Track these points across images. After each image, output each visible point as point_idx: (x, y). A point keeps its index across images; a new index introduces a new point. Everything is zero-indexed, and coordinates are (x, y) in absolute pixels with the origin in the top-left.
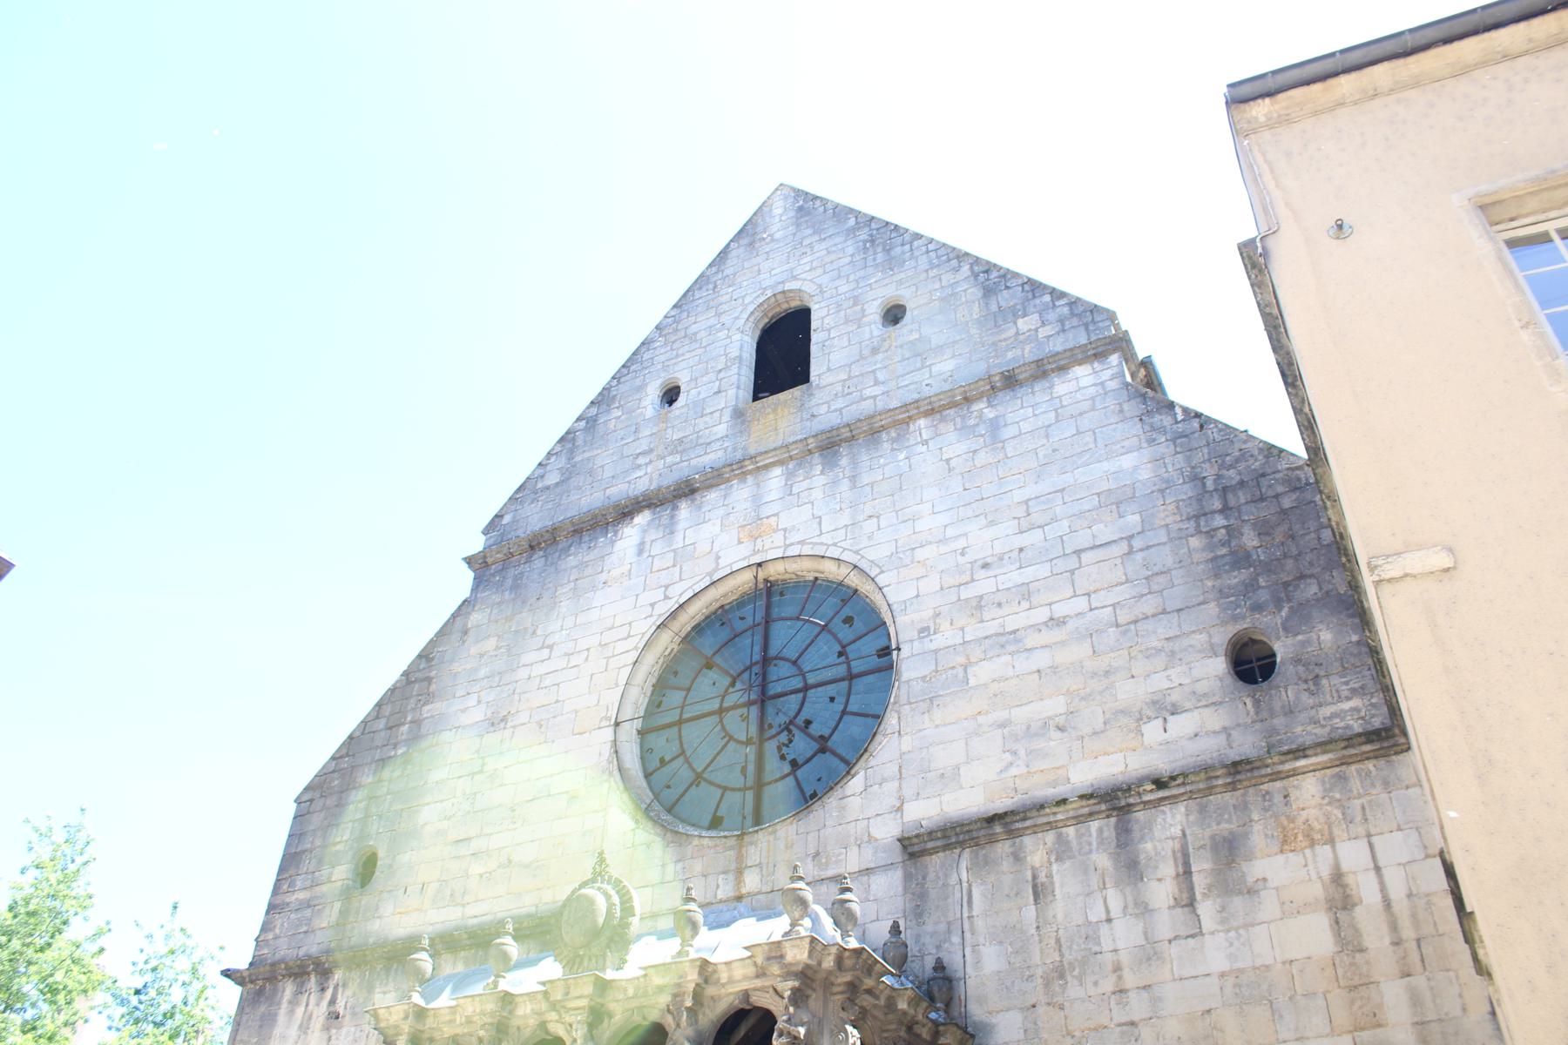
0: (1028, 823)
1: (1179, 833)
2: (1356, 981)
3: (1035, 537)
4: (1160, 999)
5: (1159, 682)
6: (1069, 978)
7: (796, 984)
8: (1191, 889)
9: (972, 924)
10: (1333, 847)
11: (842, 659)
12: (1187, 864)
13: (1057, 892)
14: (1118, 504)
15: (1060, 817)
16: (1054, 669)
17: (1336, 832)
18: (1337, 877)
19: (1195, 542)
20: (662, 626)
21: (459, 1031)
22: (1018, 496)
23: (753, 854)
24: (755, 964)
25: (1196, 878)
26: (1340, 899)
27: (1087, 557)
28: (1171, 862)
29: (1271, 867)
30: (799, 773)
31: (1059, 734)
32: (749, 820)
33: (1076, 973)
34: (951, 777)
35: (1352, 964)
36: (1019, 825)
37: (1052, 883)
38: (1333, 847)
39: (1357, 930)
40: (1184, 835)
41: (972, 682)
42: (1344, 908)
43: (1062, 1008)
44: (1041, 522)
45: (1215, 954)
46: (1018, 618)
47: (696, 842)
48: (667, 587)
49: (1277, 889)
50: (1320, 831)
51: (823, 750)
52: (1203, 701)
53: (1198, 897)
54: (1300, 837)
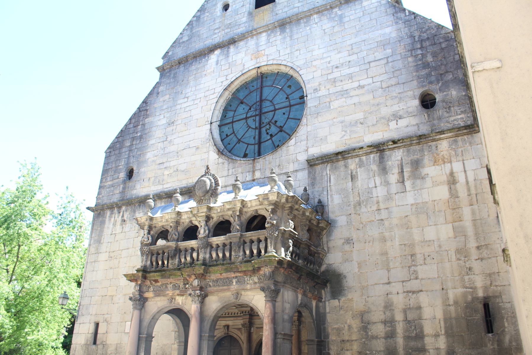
0: (350, 155)
2: (455, 207)
3: (354, 57)
5: (396, 108)
7: (273, 207)
8: (403, 177)
9: (330, 188)
10: (451, 164)
11: (287, 100)
12: (402, 169)
13: (359, 178)
14: (384, 45)
15: (360, 153)
16: (360, 103)
17: (452, 159)
18: (452, 174)
19: (410, 59)
20: (225, 89)
21: (164, 224)
22: (349, 42)
23: (258, 165)
24: (259, 201)
26: (452, 181)
27: (372, 64)
28: (397, 169)
29: (430, 170)
30: (273, 138)
31: (361, 125)
32: (257, 154)
33: (364, 204)
34: (324, 140)
35: (454, 202)
36: (346, 156)
38: (451, 164)
39: (457, 191)
40: (402, 159)
41: (332, 107)
42: (453, 184)
43: (359, 215)
44: (356, 52)
45: (410, 198)
46: (348, 85)
47: (239, 162)
48: (227, 76)
49: (431, 177)
51: (281, 131)
52: (410, 114)
53: (405, 180)
54: (440, 160)
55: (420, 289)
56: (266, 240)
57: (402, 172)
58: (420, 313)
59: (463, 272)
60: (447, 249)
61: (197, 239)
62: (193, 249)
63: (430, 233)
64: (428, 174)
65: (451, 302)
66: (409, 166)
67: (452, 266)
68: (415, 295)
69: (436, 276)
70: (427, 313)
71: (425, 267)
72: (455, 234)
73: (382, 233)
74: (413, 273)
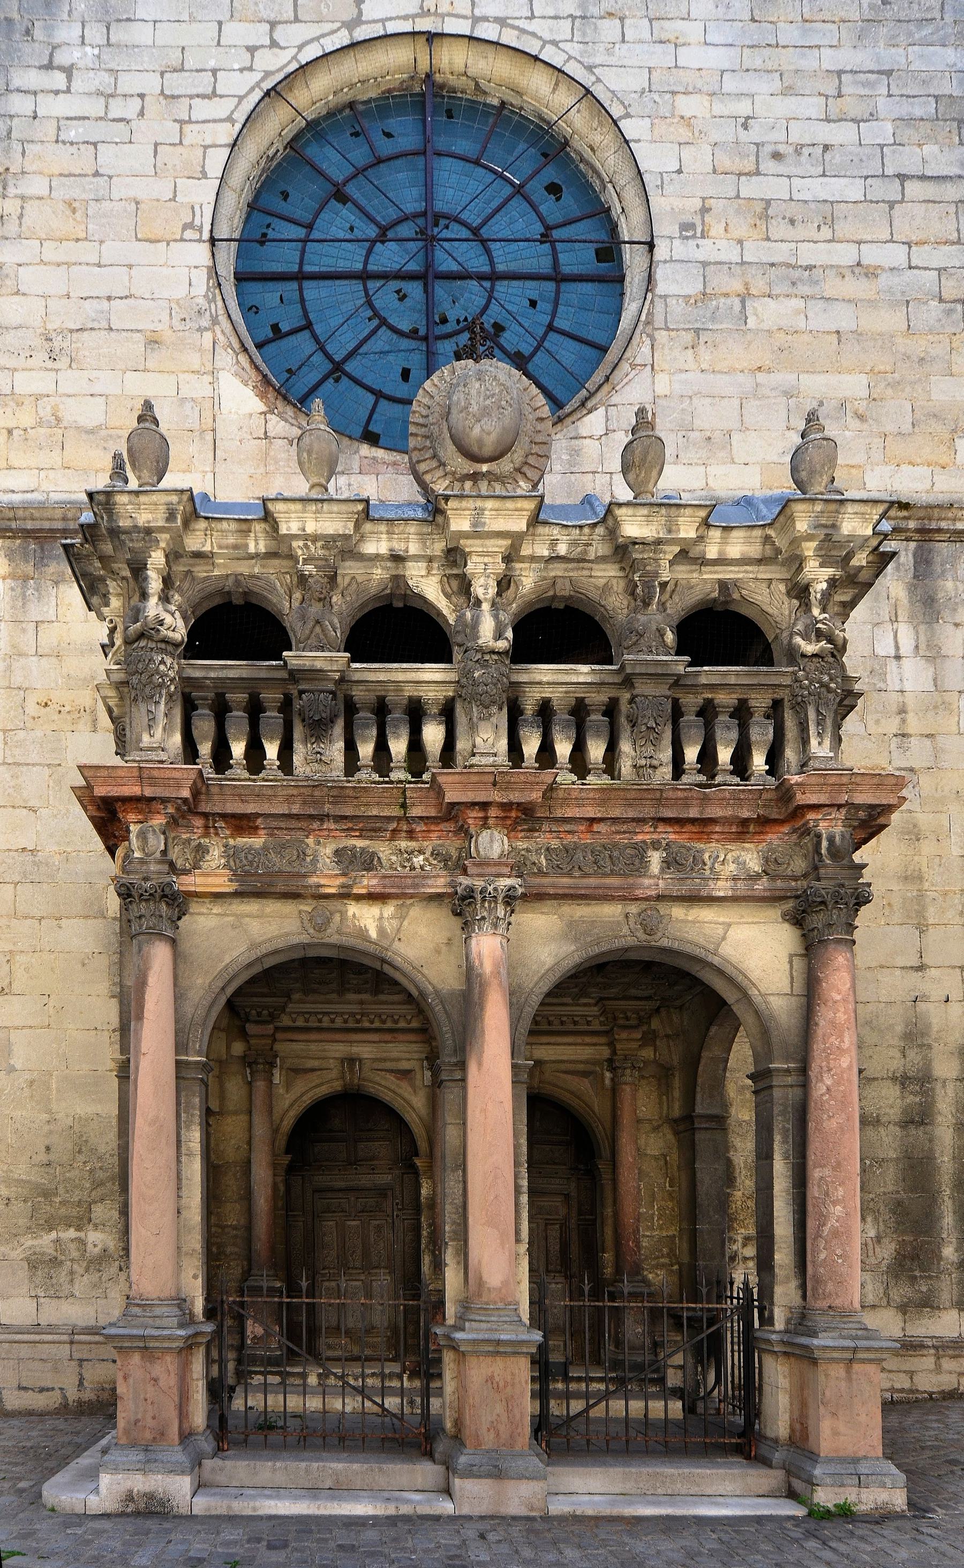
3: (843, 134)
16: (858, 334)
22: (831, 59)
27: (914, 189)
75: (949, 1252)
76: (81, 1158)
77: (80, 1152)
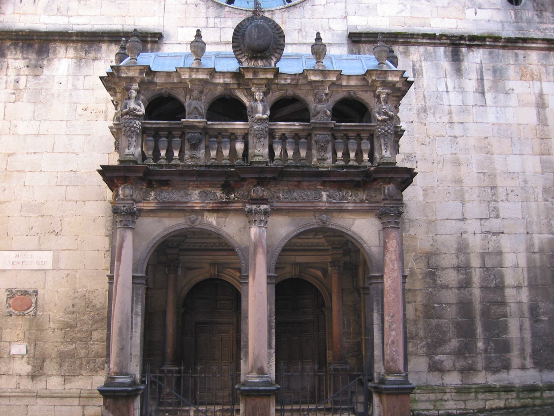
1: (480, 62)
2: (543, 137)
4: (467, 129)
6: (429, 113)
8: (483, 86)
10: (541, 83)
12: (482, 75)
13: (424, 74)
17: (543, 77)
18: (541, 95)
25: (485, 82)
26: (541, 104)
29: (515, 84)
34: (371, 9)
35: (543, 130)
37: (422, 70)
38: (541, 83)
39: (546, 117)
40: (481, 63)
42: (542, 108)
43: (425, 125)
49: (517, 94)
50: (536, 75)
53: (486, 91)
54: (528, 76)
55: (502, 230)
56: (371, 138)
57: (482, 79)
58: (501, 260)
59: (550, 216)
60: (533, 185)
61: (247, 120)
62: (232, 137)
63: (514, 164)
64: (513, 90)
65: (536, 250)
66: (490, 73)
67: (538, 206)
68: (494, 238)
69: (520, 217)
70: (509, 259)
71: (507, 204)
72: (542, 169)
73: (456, 154)
74: (493, 211)
75: (480, 345)
76: (88, 309)
77: (88, 307)
